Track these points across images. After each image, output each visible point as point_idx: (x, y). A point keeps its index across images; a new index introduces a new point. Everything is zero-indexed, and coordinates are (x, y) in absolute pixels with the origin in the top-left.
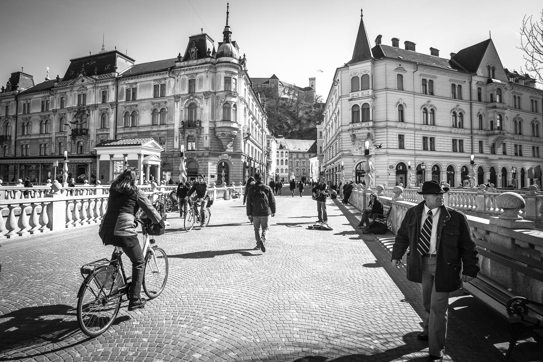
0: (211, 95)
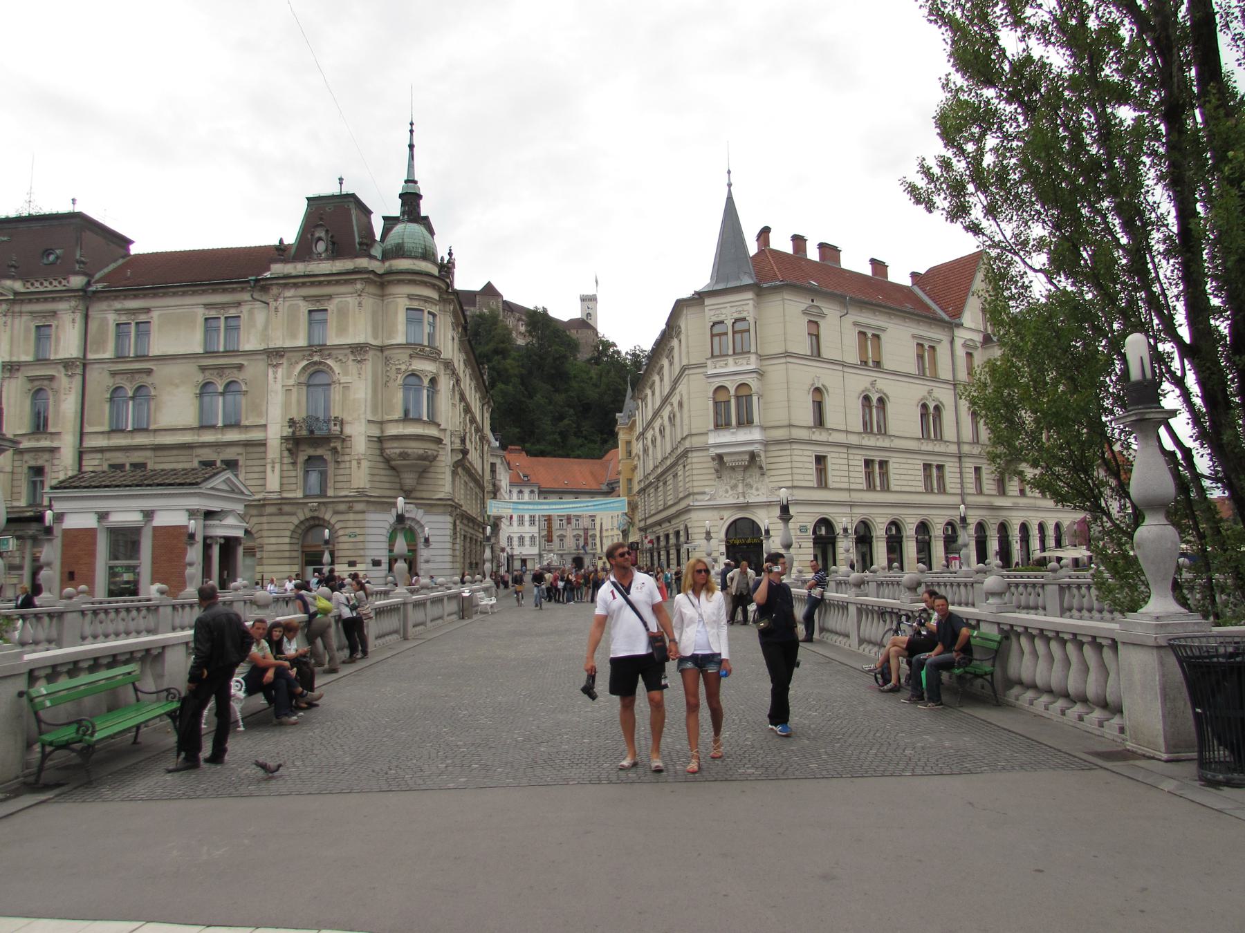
0: (371, 353)
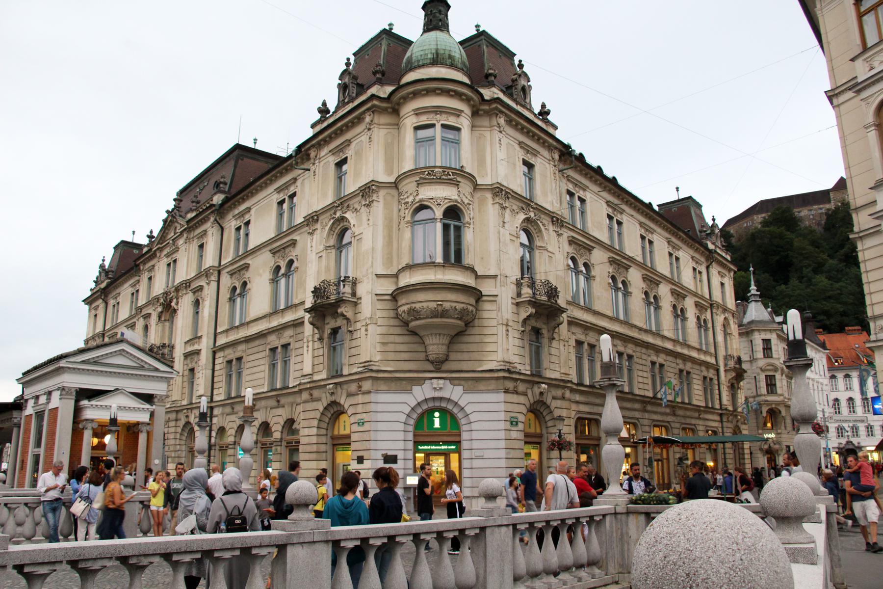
0: (382, 193)
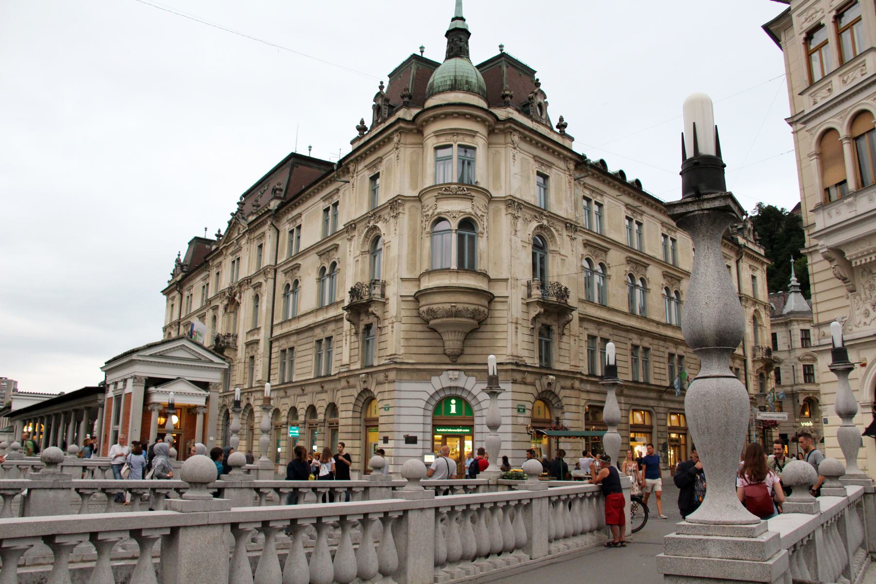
0: (408, 206)
